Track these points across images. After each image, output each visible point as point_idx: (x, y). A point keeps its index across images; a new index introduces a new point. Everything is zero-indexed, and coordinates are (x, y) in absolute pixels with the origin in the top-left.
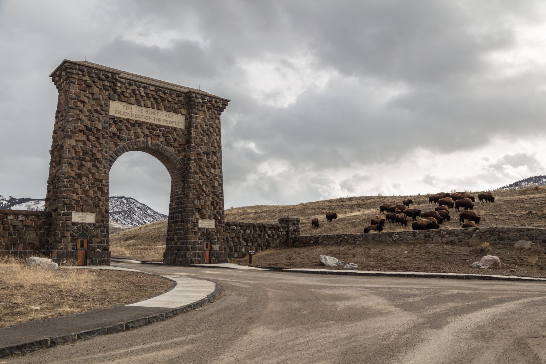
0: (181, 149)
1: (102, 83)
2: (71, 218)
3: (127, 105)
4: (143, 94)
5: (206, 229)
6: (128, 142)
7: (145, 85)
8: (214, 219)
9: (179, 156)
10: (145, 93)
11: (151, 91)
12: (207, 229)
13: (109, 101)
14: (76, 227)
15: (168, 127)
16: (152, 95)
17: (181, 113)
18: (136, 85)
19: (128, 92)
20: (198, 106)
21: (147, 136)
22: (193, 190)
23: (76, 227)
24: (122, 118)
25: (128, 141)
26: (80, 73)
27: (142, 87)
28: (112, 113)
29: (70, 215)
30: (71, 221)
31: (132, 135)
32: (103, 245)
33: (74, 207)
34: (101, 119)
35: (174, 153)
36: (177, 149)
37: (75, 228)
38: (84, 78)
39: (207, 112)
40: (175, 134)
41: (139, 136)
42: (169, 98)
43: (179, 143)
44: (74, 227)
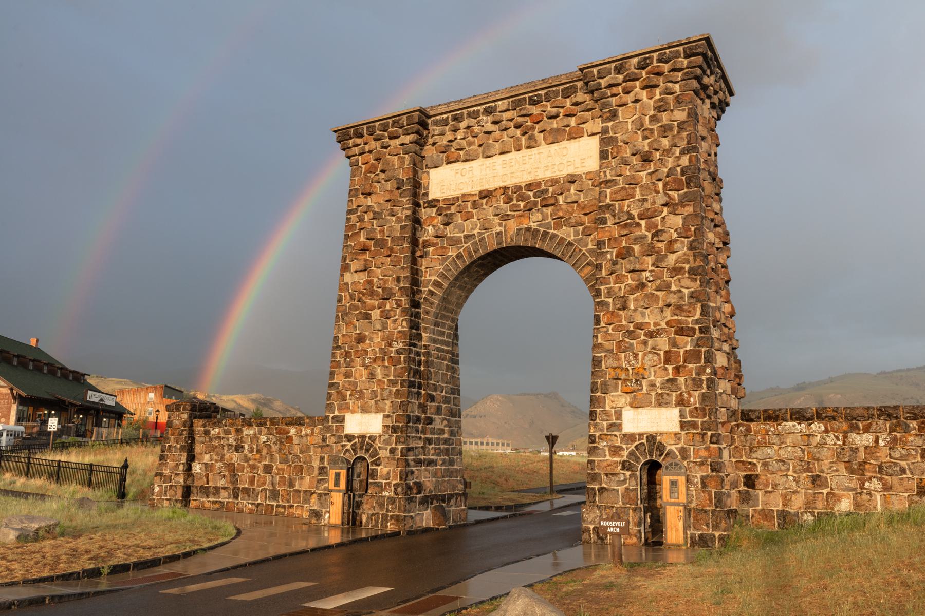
0: (589, 225)
1: (397, 142)
2: (343, 426)
3: (462, 167)
4: (490, 127)
5: (647, 437)
6: (466, 246)
7: (487, 105)
8: (676, 406)
9: (587, 245)
10: (495, 123)
11: (504, 114)
12: (651, 438)
13: (428, 173)
14: (350, 444)
15: (554, 181)
16: (511, 120)
17: (588, 133)
18: (469, 115)
19: (459, 137)
20: (614, 95)
21: (506, 218)
22: (605, 329)
23: (350, 444)
24: (449, 199)
25: (465, 243)
26: (359, 141)
27: (483, 114)
28: (435, 193)
29: (340, 420)
30: (343, 431)
31: (473, 229)
32: (394, 482)
33: (348, 404)
34: (400, 215)
35: (575, 241)
36: (581, 228)
37: (349, 447)
38: (367, 148)
39: (645, 99)
40: (572, 191)
41: (486, 225)
42: (549, 109)
43: (583, 212)
44: (347, 445)
